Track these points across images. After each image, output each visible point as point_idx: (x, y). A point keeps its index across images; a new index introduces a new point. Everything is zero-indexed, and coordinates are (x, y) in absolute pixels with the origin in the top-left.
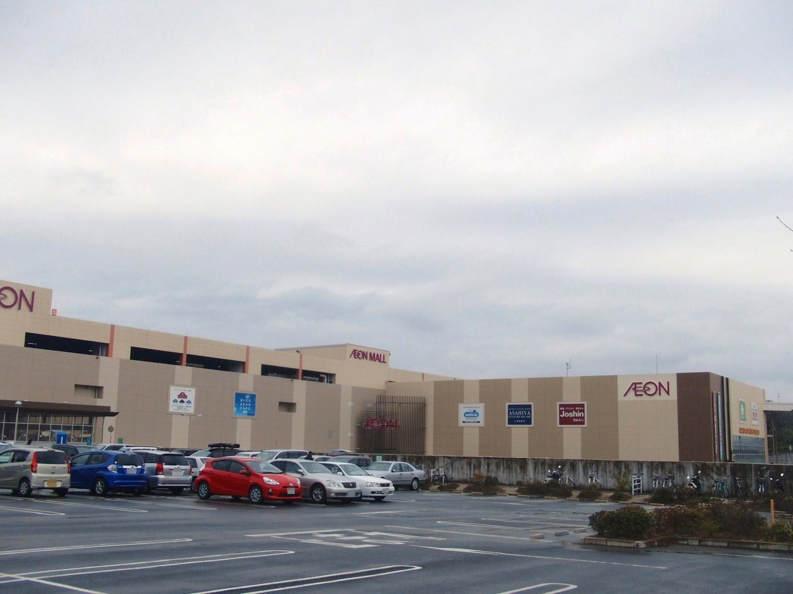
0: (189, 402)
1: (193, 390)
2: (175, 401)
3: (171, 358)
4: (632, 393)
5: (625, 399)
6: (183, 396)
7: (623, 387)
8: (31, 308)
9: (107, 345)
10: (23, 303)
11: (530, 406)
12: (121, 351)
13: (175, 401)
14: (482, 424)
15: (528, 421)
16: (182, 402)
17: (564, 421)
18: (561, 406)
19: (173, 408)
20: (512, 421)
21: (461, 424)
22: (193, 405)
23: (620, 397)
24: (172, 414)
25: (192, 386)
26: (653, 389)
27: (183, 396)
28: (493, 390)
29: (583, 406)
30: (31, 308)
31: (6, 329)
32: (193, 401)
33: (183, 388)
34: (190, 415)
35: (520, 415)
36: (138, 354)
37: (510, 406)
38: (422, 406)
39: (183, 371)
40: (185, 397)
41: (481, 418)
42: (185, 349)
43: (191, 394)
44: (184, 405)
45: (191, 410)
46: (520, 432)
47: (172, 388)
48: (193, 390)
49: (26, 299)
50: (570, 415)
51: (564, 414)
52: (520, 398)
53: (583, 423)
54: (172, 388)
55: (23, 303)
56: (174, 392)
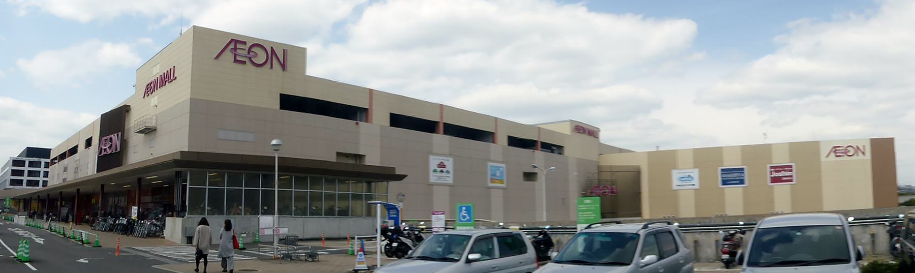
0: (448, 172)
1: (451, 159)
2: (435, 171)
3: (429, 126)
4: (833, 155)
5: (827, 160)
6: (442, 165)
7: (825, 150)
8: (283, 66)
9: (366, 110)
10: (275, 61)
11: (742, 169)
12: (380, 118)
13: (435, 171)
14: (697, 187)
15: (742, 182)
16: (442, 171)
17: (775, 180)
18: (772, 167)
19: (433, 178)
20: (725, 182)
21: (675, 187)
22: (451, 175)
23: (823, 158)
24: (432, 185)
25: (450, 155)
26: (852, 152)
27: (442, 165)
28: (705, 157)
29: (791, 166)
30: (283, 66)
31: (261, 90)
32: (451, 170)
33: (440, 157)
34: (450, 185)
35: (733, 177)
36: (397, 121)
37: (723, 170)
38: (636, 174)
39: (440, 139)
40: (444, 166)
41: (696, 181)
42: (442, 118)
43: (449, 164)
44: (444, 174)
45: (450, 180)
46: (733, 192)
47: (431, 157)
48: (451, 159)
49: (277, 58)
50: (780, 175)
51: (775, 175)
52: (731, 163)
53: (791, 181)
54: (431, 157)
55: (275, 61)
56: (434, 162)
